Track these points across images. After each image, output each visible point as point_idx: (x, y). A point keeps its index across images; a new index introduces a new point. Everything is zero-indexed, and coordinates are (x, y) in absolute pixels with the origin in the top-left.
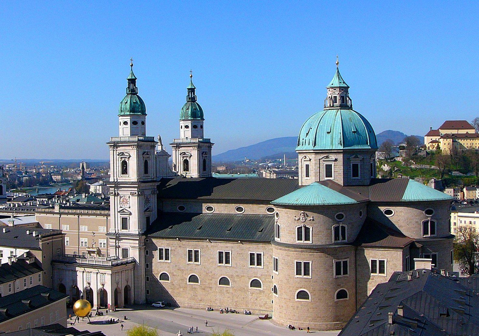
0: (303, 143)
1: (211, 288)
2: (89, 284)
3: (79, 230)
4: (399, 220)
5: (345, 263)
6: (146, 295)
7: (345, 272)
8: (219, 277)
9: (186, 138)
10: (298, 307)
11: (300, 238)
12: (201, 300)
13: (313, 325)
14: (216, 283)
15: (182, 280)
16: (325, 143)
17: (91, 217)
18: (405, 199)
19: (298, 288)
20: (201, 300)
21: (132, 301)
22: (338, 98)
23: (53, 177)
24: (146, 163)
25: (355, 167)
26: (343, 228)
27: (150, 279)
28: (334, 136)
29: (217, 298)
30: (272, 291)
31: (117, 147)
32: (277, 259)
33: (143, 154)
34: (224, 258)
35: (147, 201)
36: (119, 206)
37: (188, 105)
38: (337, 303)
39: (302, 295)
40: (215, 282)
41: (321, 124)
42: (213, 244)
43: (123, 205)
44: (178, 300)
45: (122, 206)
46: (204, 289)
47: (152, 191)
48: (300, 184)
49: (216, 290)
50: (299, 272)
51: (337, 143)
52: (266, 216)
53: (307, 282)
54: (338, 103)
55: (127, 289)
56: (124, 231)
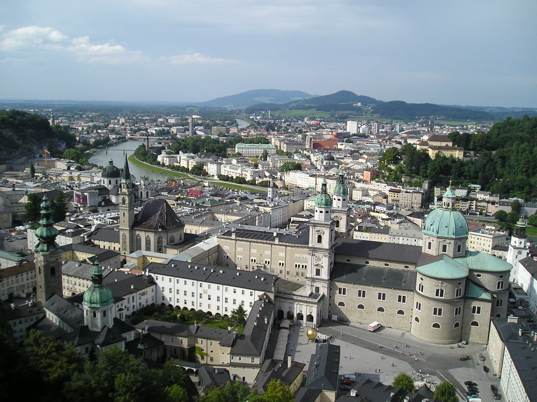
1: (372, 313)
2: (301, 311)
3: (250, 251)
5: (460, 308)
7: (459, 313)
10: (432, 332)
11: (437, 295)
16: (444, 233)
17: (259, 244)
19: (434, 322)
20: (365, 319)
22: (451, 204)
25: (459, 247)
26: (461, 289)
31: (315, 226)
34: (381, 297)
36: (315, 262)
37: (340, 186)
39: (436, 326)
41: (441, 221)
42: (375, 288)
44: (350, 318)
50: (435, 313)
51: (451, 234)
52: (403, 270)
54: (450, 207)
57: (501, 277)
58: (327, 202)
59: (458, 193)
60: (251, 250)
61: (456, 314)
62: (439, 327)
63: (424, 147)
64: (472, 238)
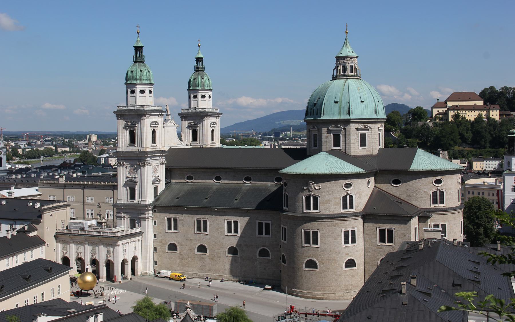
0: (311, 112)
1: (219, 257)
4: (407, 190)
5: (353, 232)
6: (154, 266)
7: (354, 241)
8: (227, 247)
9: (194, 108)
11: (308, 207)
12: (209, 270)
13: (322, 294)
14: (224, 252)
15: (190, 250)
18: (414, 168)
20: (209, 270)
21: (140, 273)
23: (58, 149)
24: (154, 132)
25: (363, 138)
26: (351, 197)
27: (158, 249)
28: (343, 106)
29: (225, 267)
30: (281, 260)
32: (285, 229)
33: (151, 124)
35: (155, 171)
38: (346, 272)
40: (224, 251)
43: (130, 175)
45: (128, 176)
46: (212, 259)
47: (160, 161)
48: (308, 153)
49: (224, 259)
50: (307, 242)
51: (345, 112)
53: (315, 251)
55: (134, 260)
56: (132, 202)
57: (438, 182)
58: (141, 75)
59: (487, 166)
60: (86, 199)
61: (346, 242)
62: (317, 268)
63: (441, 110)
64: (469, 193)
